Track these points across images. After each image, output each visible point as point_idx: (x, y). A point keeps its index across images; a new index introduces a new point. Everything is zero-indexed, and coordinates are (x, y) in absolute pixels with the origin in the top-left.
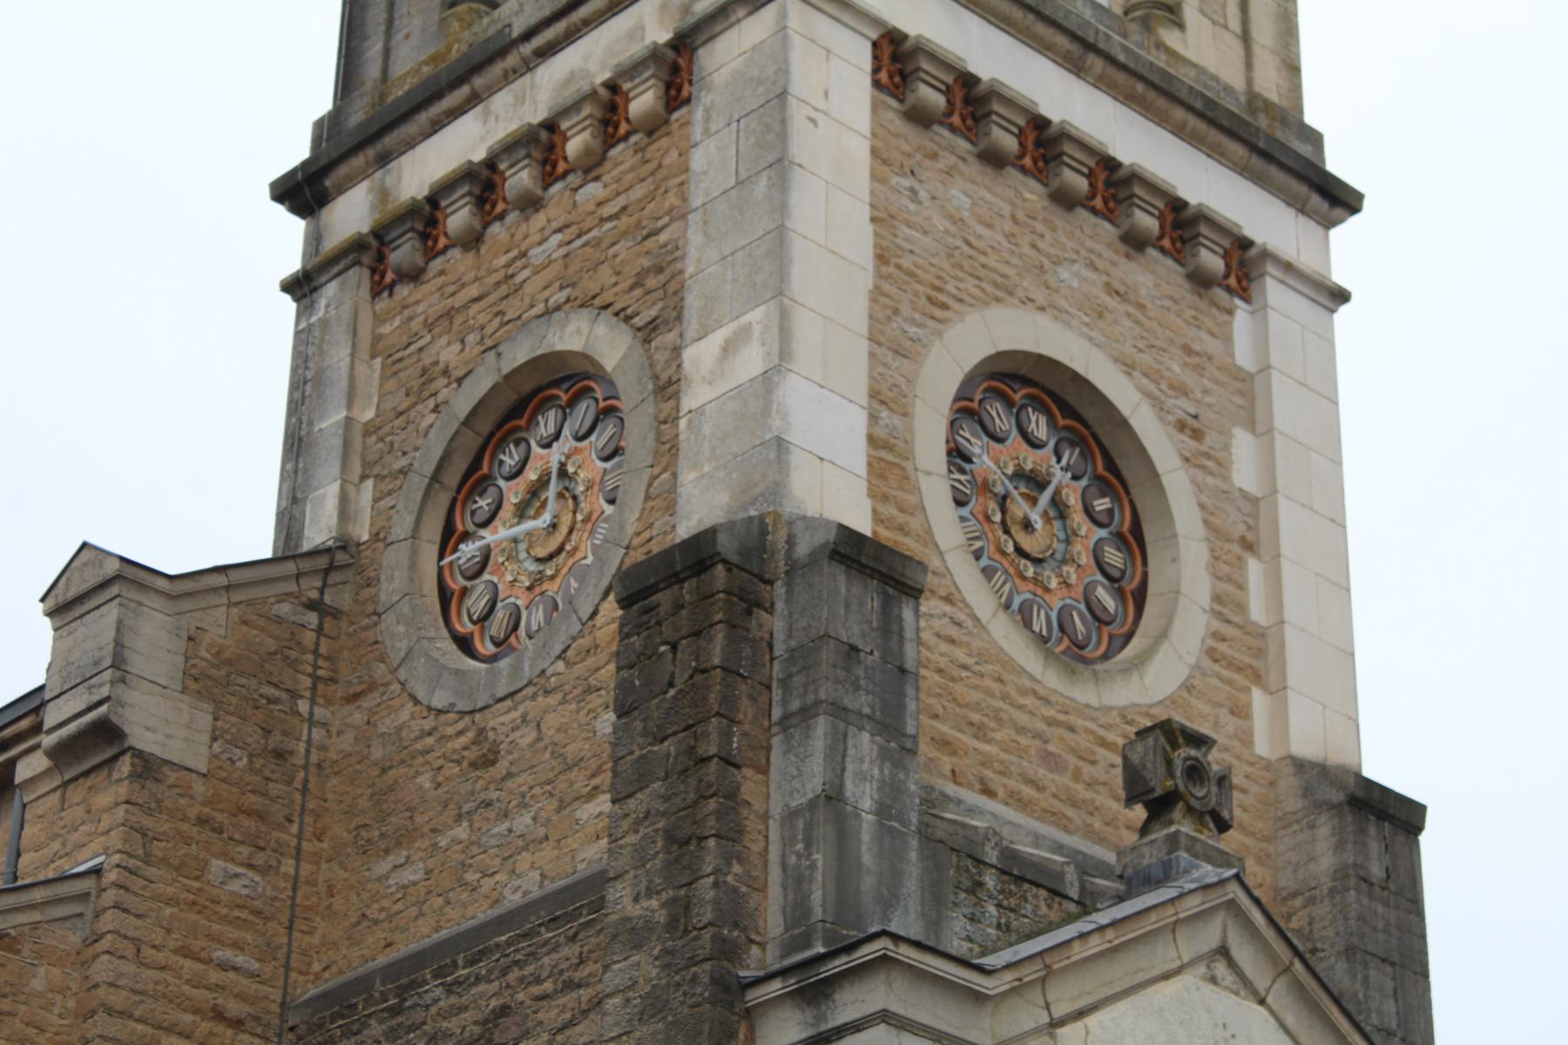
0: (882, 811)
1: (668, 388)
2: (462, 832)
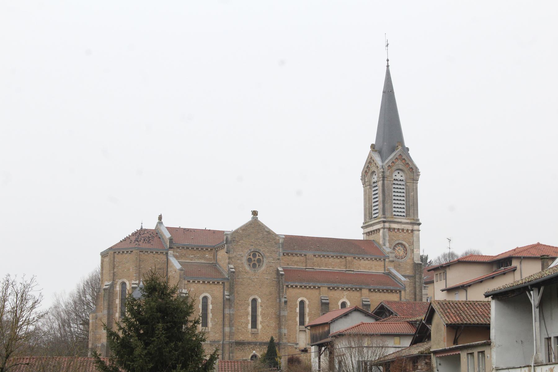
1: (413, 251)
2: (398, 268)
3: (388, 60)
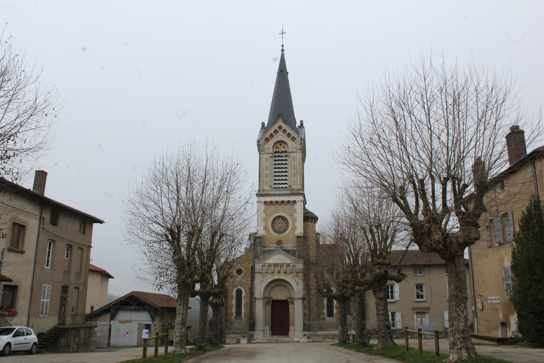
0: (260, 251)
3: (283, 46)
